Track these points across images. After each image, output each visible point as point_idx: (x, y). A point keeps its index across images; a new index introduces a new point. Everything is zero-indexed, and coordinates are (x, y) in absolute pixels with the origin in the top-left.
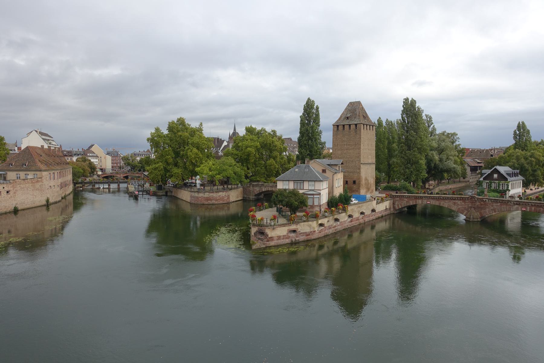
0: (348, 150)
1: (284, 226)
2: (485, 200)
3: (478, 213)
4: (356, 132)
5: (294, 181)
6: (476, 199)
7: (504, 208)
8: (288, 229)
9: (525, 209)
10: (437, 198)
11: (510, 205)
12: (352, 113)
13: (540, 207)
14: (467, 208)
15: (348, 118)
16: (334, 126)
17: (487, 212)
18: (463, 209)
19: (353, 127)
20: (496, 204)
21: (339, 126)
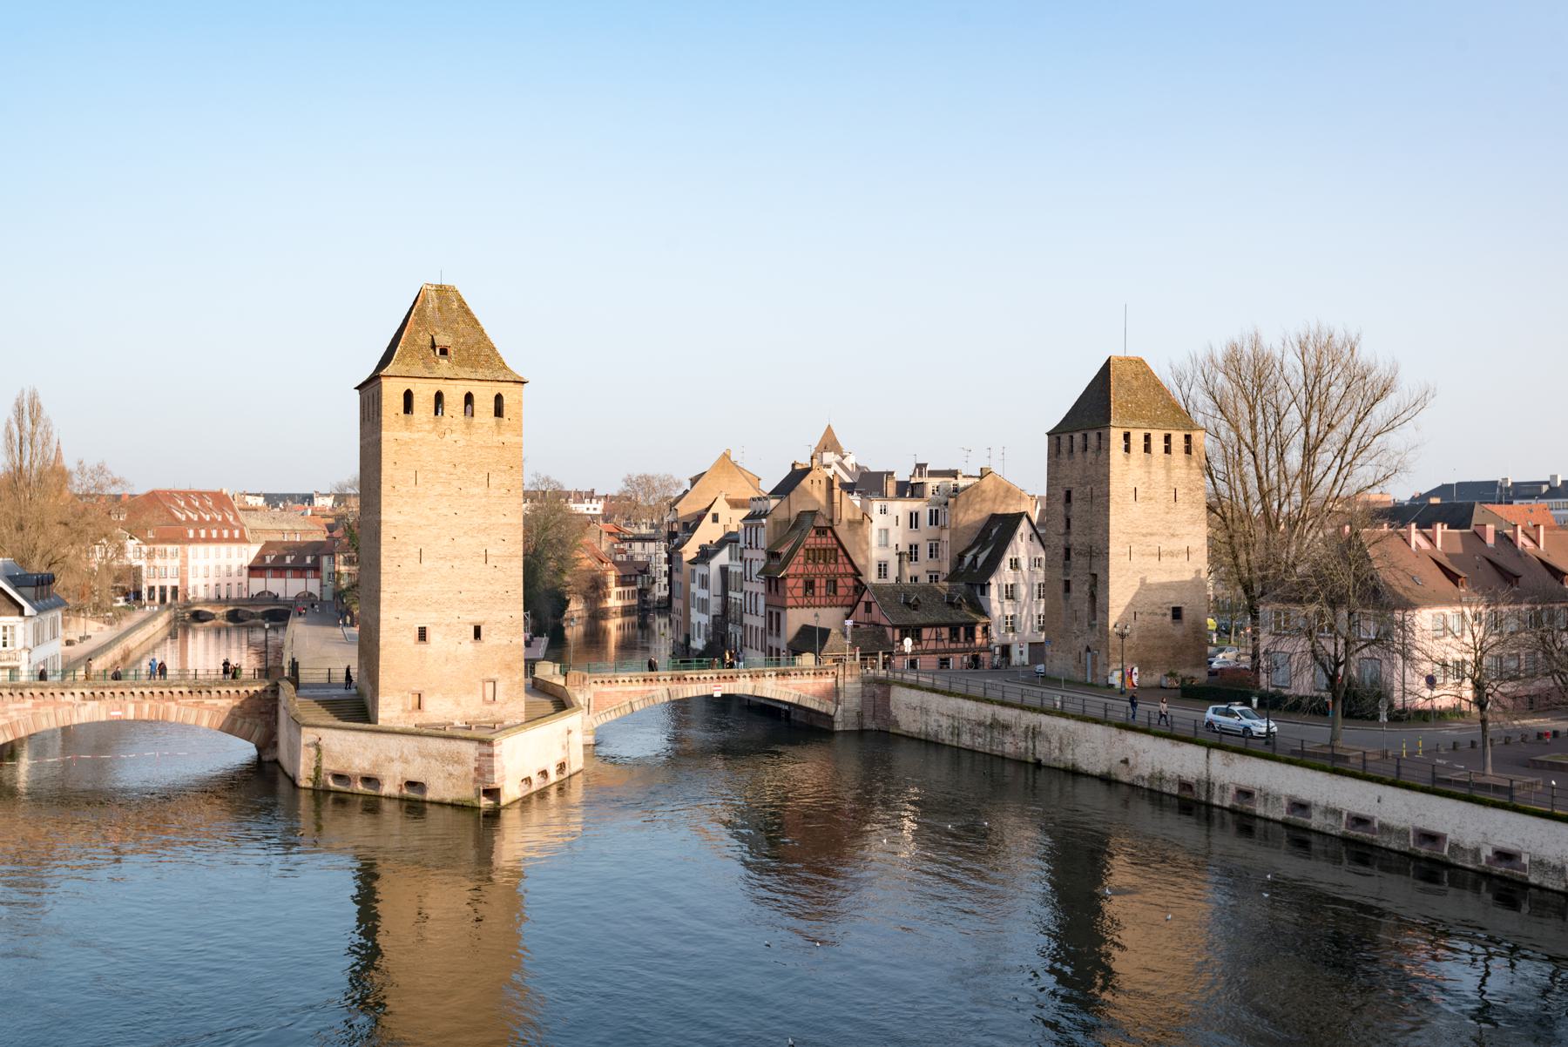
7: (47, 715)
9: (119, 713)
11: (70, 703)
13: (169, 700)
20: (18, 706)
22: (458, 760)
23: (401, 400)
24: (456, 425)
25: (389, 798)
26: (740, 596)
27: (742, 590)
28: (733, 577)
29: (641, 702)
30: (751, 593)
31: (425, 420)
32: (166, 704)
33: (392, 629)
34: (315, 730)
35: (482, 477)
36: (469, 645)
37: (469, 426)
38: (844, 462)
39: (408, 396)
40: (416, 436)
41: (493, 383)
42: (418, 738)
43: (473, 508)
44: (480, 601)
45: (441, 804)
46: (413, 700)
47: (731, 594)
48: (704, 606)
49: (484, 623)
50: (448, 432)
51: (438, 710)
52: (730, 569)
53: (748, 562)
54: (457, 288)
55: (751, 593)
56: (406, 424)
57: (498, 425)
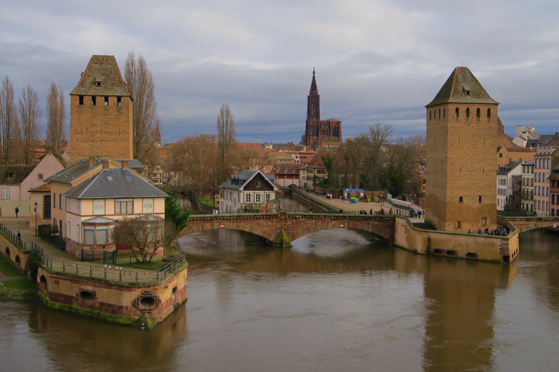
0: (103, 142)
1: (170, 282)
2: (297, 217)
3: (289, 236)
4: (119, 110)
5: (115, 199)
6: (287, 216)
8: (173, 287)
10: (235, 218)
11: (327, 221)
12: (103, 74)
14: (275, 230)
15: (99, 84)
16: (74, 97)
17: (300, 232)
18: (270, 232)
19: (113, 101)
20: (310, 222)
21: (85, 98)
22: (493, 245)
23: (455, 111)
24: (474, 120)
25: (461, 259)
26: (533, 188)
27: (532, 186)
28: (526, 180)
29: (525, 229)
30: (539, 187)
31: (463, 119)
32: (358, 223)
33: (450, 197)
34: (427, 233)
35: (482, 141)
36: (477, 204)
37: (478, 121)
38: (530, 130)
39: (457, 110)
40: (460, 125)
41: (486, 105)
42: (474, 237)
43: (479, 152)
44: (481, 188)
45: (485, 261)
46: (457, 224)
47: (523, 187)
48: (502, 192)
49: (483, 196)
50: (471, 123)
51: (466, 227)
52: (523, 177)
53: (538, 174)
54: (468, 68)
55: (539, 187)
56: (456, 121)
57: (489, 120)
